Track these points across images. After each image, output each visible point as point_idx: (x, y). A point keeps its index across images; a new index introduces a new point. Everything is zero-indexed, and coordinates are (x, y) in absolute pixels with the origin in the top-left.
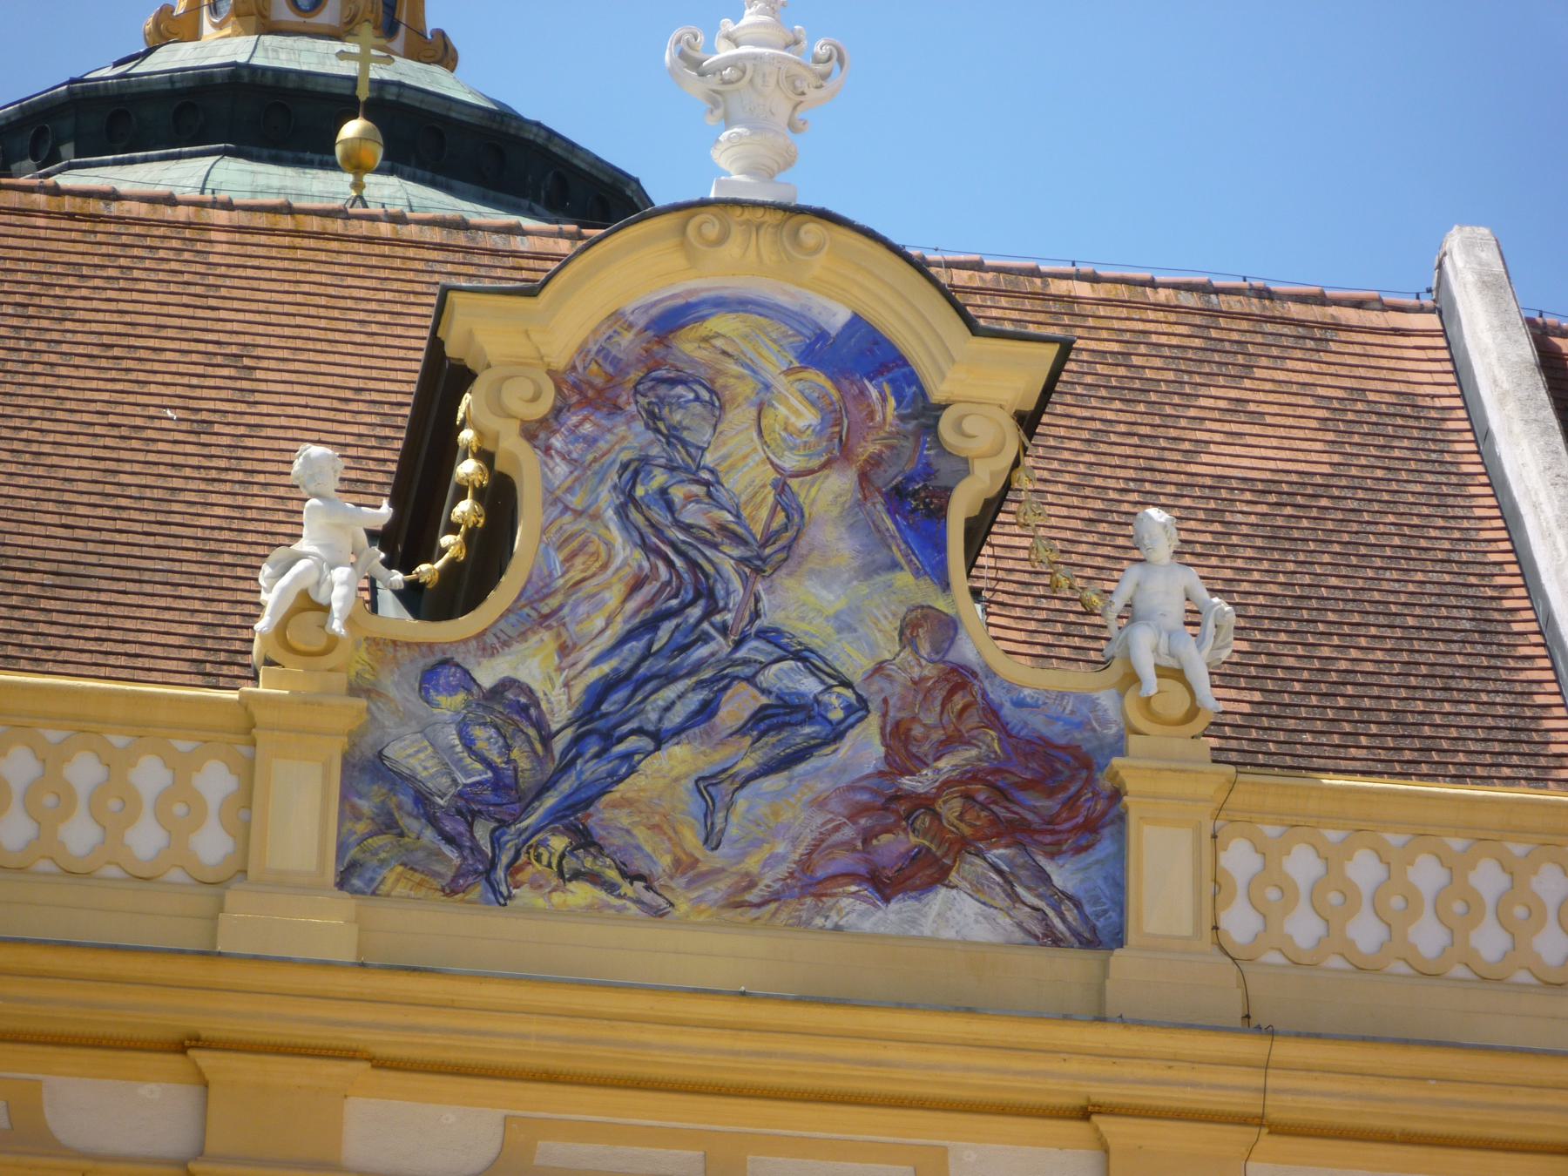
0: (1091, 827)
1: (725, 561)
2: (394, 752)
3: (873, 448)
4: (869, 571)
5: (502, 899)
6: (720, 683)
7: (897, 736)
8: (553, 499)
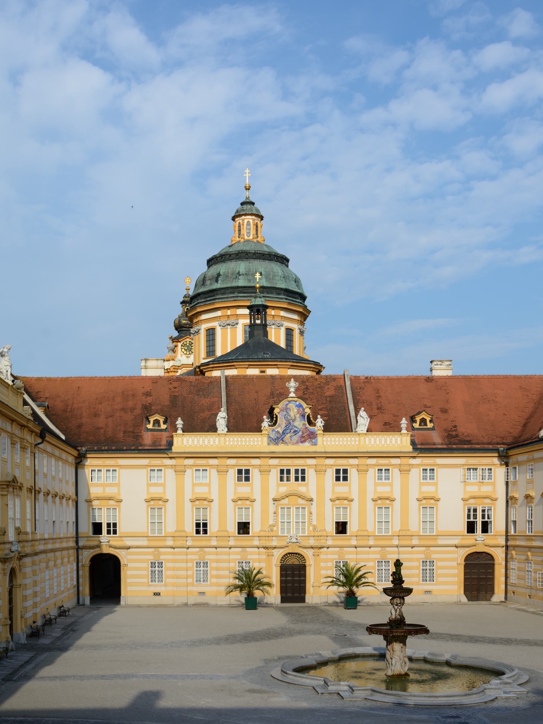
0: (315, 437)
1: (291, 421)
2: (271, 436)
3: (300, 412)
4: (300, 421)
5: (278, 445)
6: (291, 430)
7: (303, 432)
8: (280, 418)
